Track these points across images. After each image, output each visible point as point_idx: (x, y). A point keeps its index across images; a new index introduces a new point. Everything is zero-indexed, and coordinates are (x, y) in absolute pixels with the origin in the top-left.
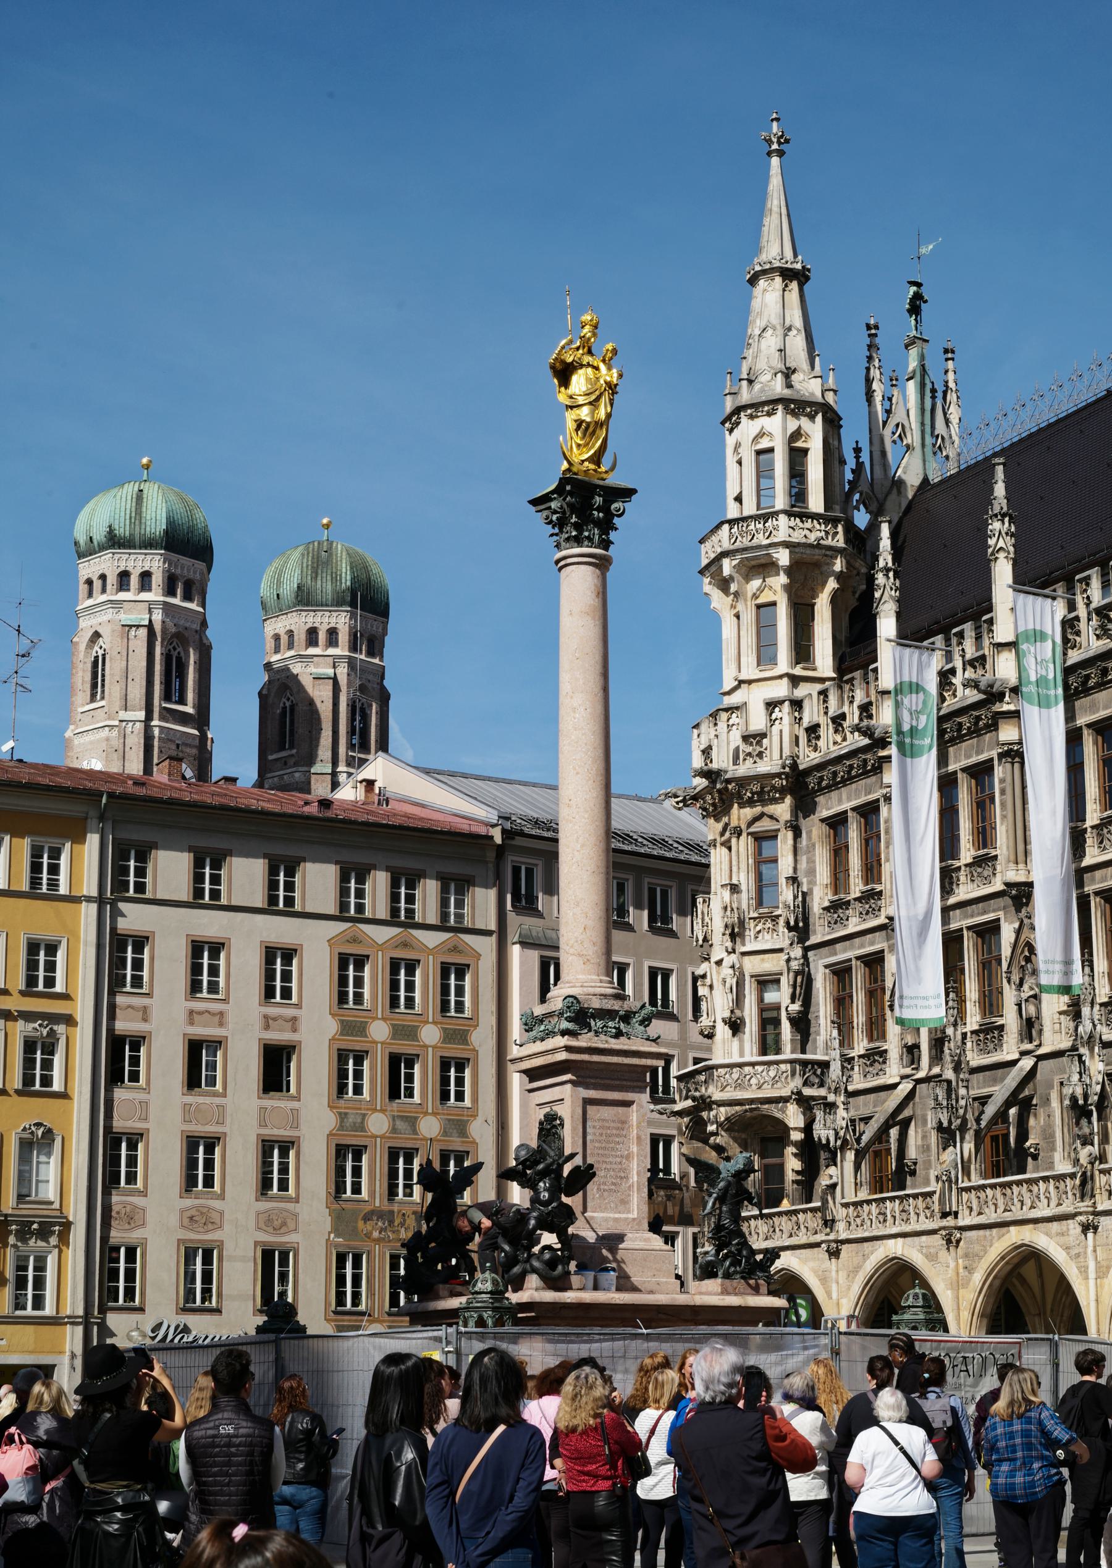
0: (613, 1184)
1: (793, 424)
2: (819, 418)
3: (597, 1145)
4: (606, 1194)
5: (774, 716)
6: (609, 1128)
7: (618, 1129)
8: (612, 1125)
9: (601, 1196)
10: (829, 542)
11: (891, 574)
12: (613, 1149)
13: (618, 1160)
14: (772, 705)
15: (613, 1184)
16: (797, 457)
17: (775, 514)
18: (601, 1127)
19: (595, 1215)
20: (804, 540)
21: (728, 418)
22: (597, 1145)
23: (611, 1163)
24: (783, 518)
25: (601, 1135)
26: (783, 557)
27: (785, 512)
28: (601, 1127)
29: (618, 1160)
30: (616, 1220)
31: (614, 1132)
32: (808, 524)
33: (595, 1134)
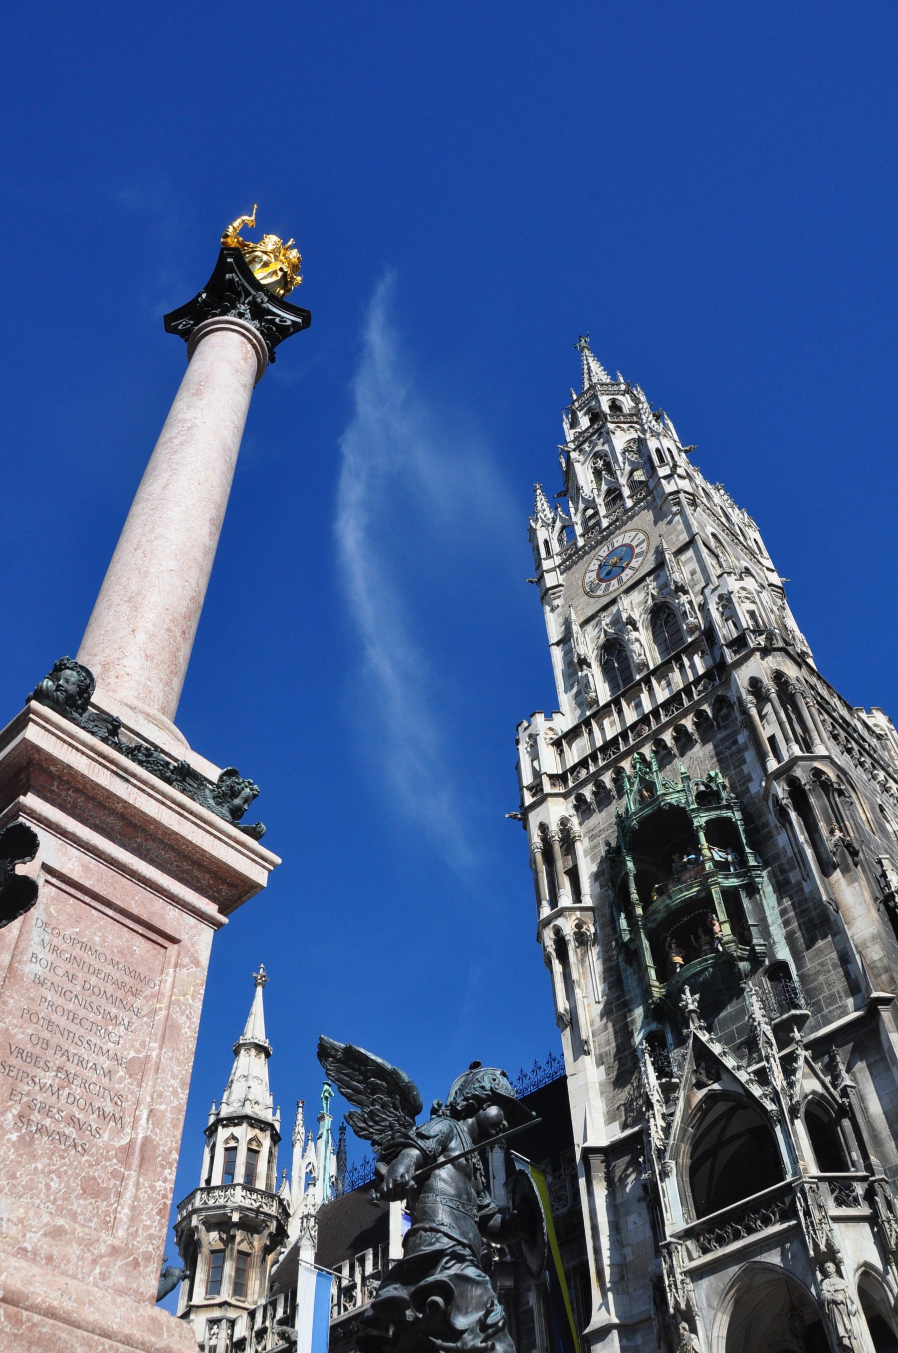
0: (72, 1120)
1: (252, 1133)
2: (268, 1133)
4: (42, 1143)
5: (212, 1332)
6: (96, 972)
9: (25, 1143)
10: (265, 1209)
11: (312, 1220)
14: (213, 1322)
15: (72, 1120)
16: (253, 1153)
17: (234, 1186)
20: (250, 1206)
21: (209, 1128)
24: (239, 1188)
26: (236, 1217)
27: (239, 1184)
29: (107, 1064)
30: (56, 1233)
31: (110, 989)
32: (254, 1196)
33: (53, 968)
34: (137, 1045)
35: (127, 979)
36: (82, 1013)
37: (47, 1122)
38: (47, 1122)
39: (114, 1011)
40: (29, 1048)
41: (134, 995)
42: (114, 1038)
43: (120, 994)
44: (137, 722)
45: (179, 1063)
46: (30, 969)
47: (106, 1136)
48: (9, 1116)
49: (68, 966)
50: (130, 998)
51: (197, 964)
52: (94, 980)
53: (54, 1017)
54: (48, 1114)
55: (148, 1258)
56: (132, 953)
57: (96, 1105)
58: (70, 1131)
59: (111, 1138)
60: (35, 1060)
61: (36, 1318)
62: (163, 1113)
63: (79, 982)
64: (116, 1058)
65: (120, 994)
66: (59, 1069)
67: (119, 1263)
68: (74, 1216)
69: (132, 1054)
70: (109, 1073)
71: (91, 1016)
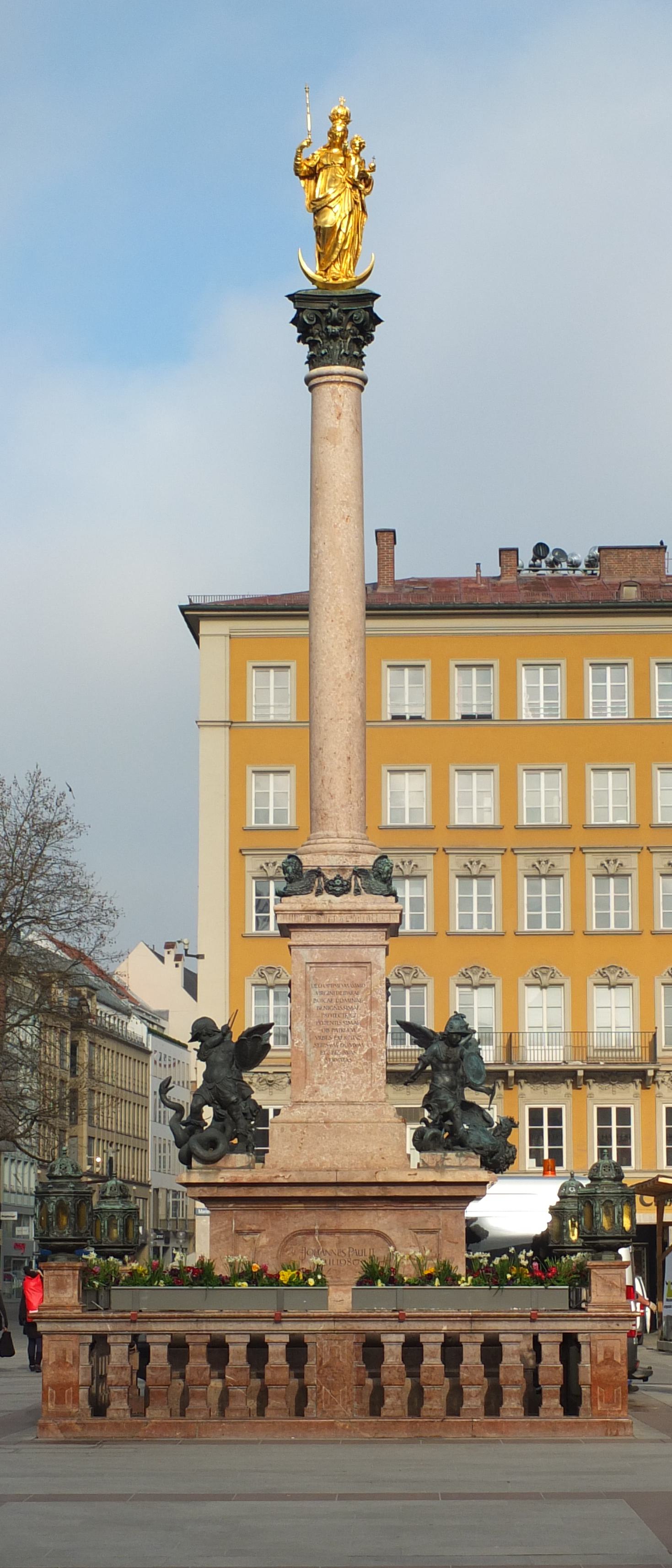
0: (344, 1052)
3: (325, 1012)
6: (340, 993)
7: (351, 993)
8: (344, 989)
12: (345, 1015)
13: (352, 1026)
18: (329, 993)
19: (321, 1087)
22: (325, 1012)
23: (342, 1030)
25: (331, 1001)
28: (333, 993)
29: (352, 1026)
31: (347, 997)
33: (323, 1000)
34: (363, 1014)
35: (353, 989)
36: (338, 1012)
37: (336, 1056)
38: (336, 1056)
39: (350, 1005)
40: (323, 1034)
41: (357, 994)
42: (353, 1015)
43: (351, 997)
44: (328, 860)
45: (379, 1015)
46: (315, 1005)
47: (358, 1052)
48: (322, 1060)
49: (328, 997)
50: (356, 996)
51: (380, 968)
52: (340, 997)
53: (328, 1019)
54: (335, 1054)
55: (380, 1088)
56: (352, 976)
57: (352, 1043)
58: (345, 1056)
59: (360, 1051)
60: (326, 1038)
61: (335, 1124)
62: (376, 1037)
63: (334, 1001)
64: (356, 1023)
65: (351, 997)
66: (335, 1037)
67: (370, 1093)
68: (353, 1083)
69: (361, 1018)
70: (354, 1030)
71: (342, 1012)
